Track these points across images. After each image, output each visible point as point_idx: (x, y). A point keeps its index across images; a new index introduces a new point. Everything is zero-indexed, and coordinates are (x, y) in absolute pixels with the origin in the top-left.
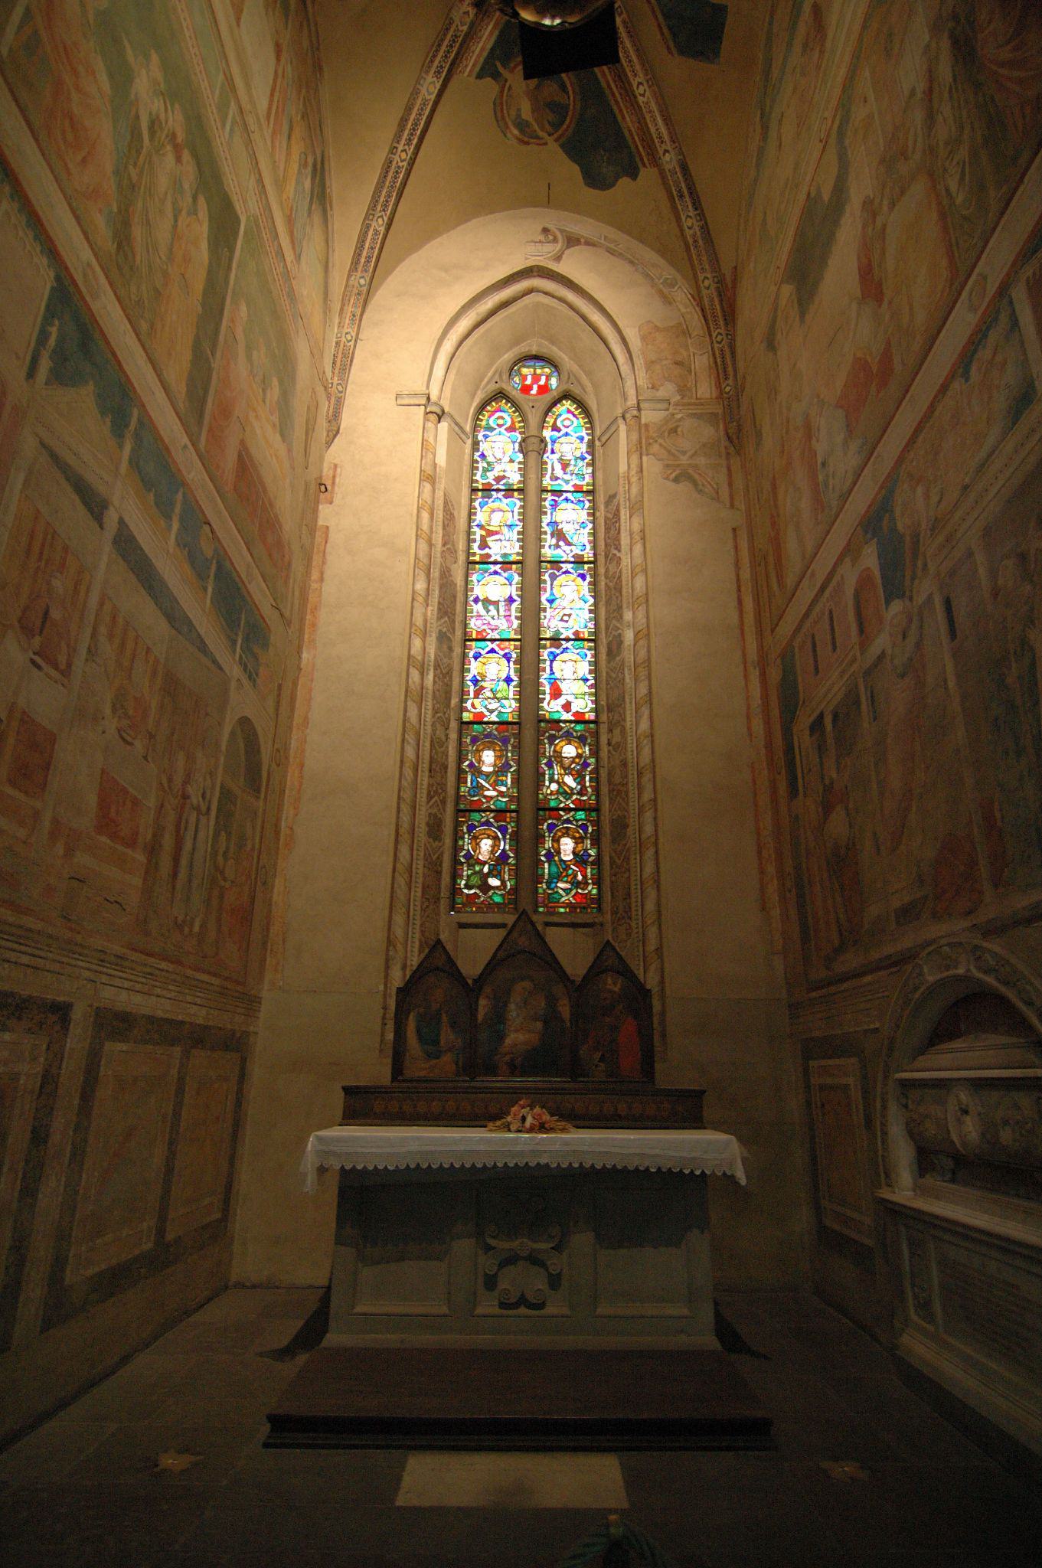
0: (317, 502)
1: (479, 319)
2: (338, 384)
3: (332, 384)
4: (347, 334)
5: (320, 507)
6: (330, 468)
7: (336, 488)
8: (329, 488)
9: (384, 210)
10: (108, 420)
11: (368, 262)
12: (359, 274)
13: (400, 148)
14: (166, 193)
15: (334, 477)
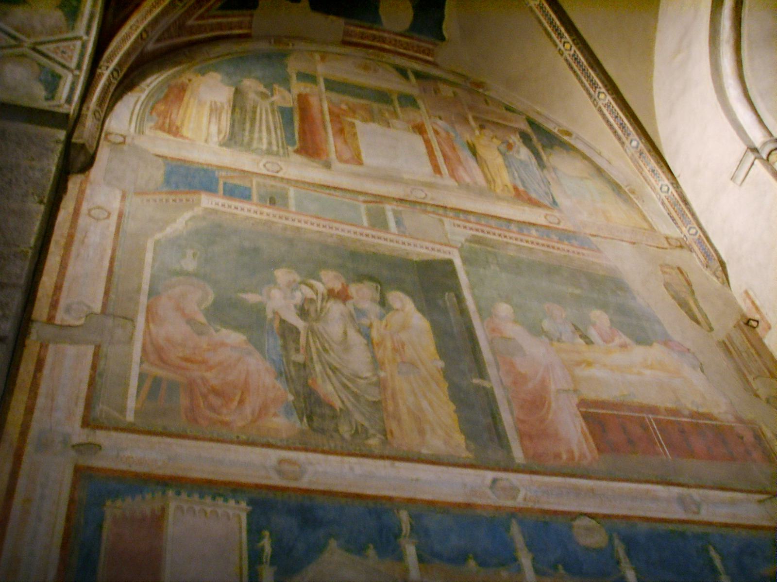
0: (760, 340)
1: (732, 42)
2: (689, 231)
3: (685, 236)
4: (661, 189)
5: (766, 341)
6: (744, 300)
7: (762, 310)
8: (757, 317)
9: (596, 88)
10: (371, 552)
11: (624, 127)
12: (627, 143)
13: (561, 46)
14: (345, 333)
15: (753, 303)
